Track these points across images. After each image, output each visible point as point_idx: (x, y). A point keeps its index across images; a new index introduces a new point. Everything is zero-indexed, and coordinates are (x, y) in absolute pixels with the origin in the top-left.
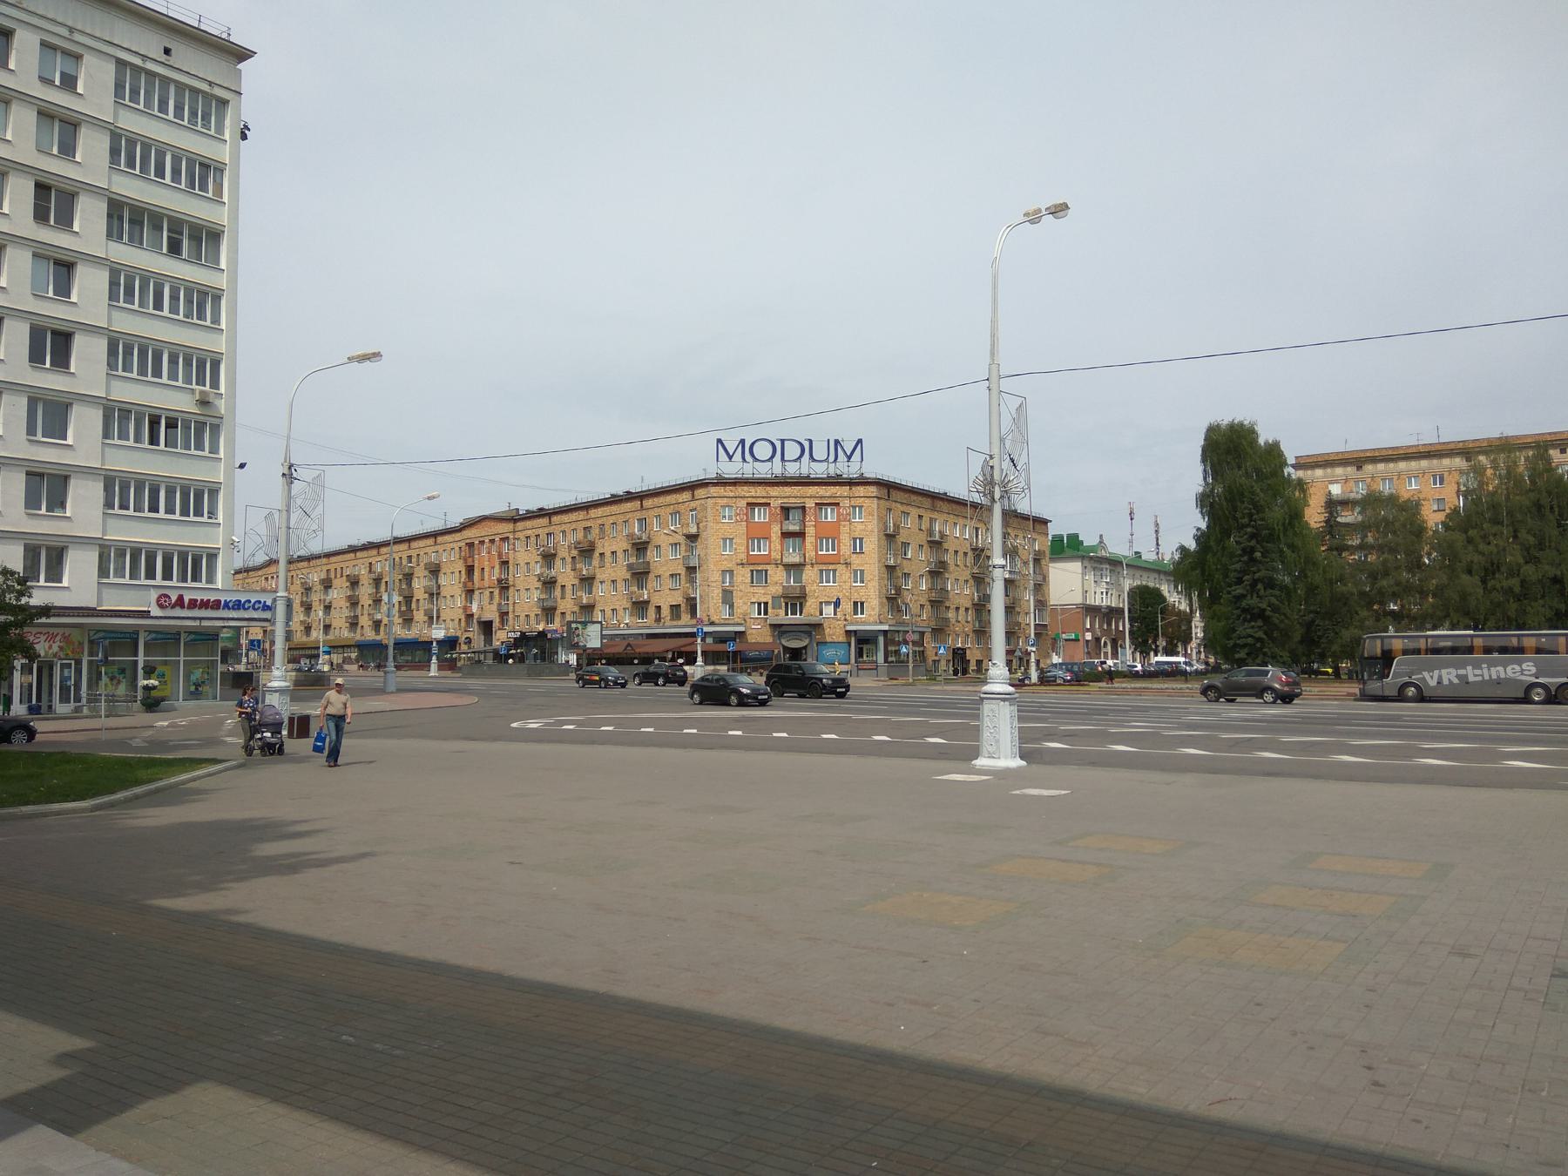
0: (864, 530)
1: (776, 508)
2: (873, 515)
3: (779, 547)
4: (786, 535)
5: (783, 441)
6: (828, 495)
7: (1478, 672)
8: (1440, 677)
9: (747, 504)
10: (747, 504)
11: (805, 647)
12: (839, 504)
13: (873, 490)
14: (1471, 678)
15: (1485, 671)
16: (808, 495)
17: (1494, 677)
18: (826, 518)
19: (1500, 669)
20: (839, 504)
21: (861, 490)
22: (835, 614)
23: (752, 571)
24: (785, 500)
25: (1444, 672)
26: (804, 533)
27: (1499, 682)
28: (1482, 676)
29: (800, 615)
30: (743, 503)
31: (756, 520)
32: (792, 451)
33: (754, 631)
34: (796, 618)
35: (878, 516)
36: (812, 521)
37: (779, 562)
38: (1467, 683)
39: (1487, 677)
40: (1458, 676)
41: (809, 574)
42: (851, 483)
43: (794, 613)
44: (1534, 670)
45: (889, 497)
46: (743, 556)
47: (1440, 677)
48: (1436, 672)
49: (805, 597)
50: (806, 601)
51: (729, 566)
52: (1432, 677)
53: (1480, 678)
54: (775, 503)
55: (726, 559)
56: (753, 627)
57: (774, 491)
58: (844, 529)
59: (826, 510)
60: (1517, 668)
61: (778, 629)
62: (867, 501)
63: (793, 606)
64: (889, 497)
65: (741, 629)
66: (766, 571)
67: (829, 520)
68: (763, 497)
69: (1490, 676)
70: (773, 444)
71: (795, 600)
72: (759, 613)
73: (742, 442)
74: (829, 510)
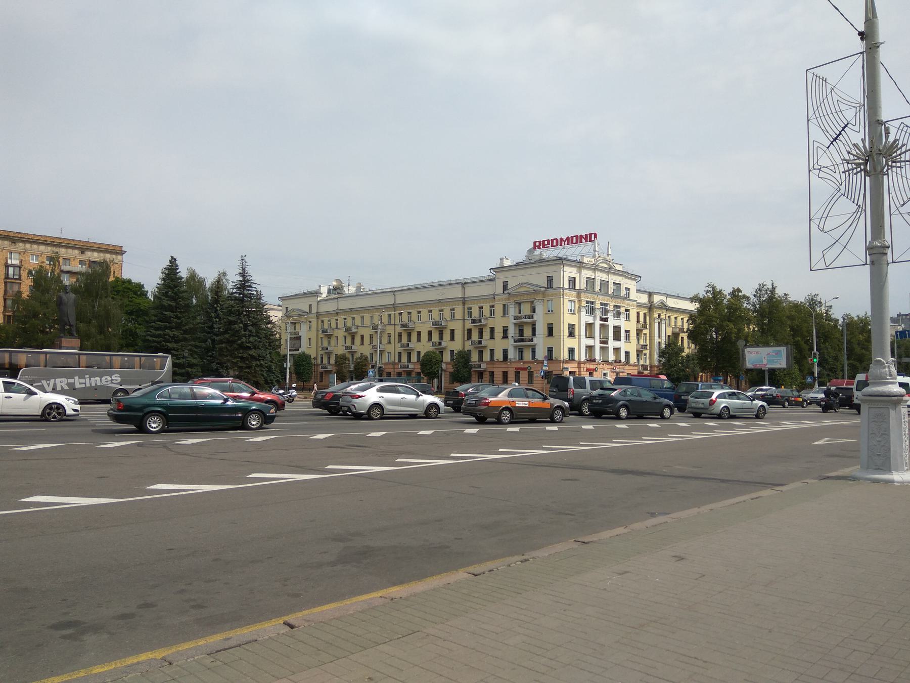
7: (82, 381)
8: (55, 384)
14: (78, 386)
15: (88, 380)
17: (93, 385)
19: (98, 379)
25: (58, 380)
27: (96, 388)
28: (85, 384)
38: (74, 389)
39: (88, 385)
40: (68, 384)
44: (119, 380)
47: (55, 384)
48: (52, 381)
52: (49, 385)
53: (83, 386)
60: (109, 379)
69: (91, 384)
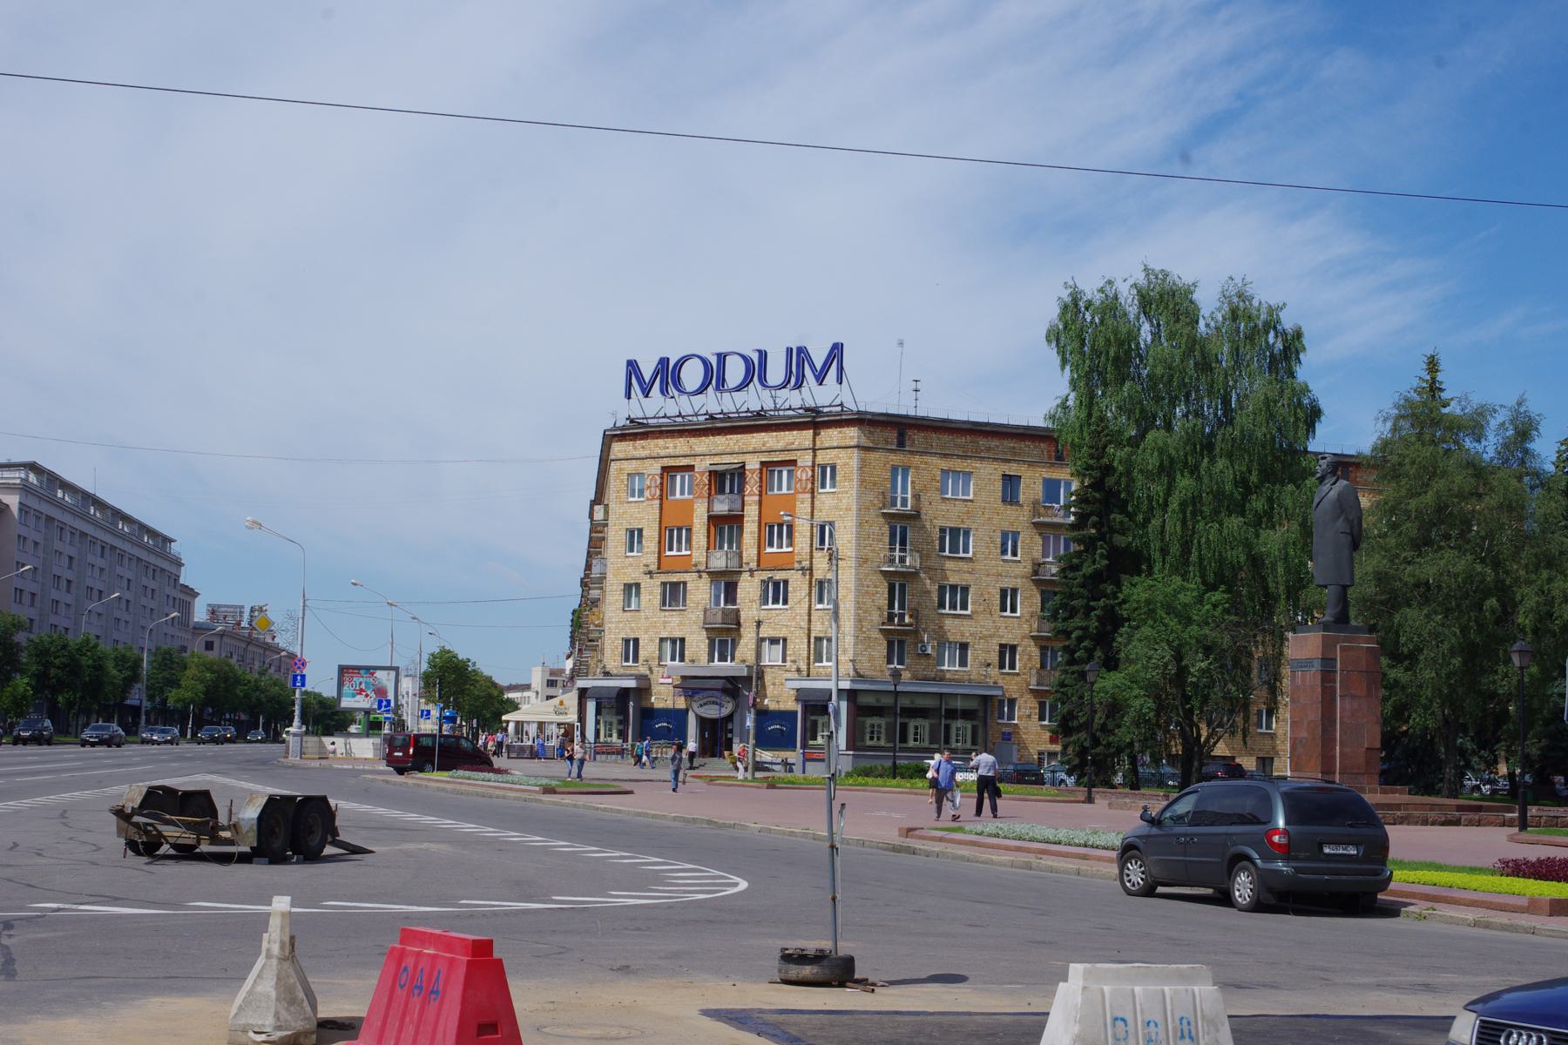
0: (837, 508)
1: (702, 474)
2: (851, 480)
3: (704, 542)
4: (715, 521)
5: (722, 358)
6: (780, 445)
9: (664, 468)
10: (664, 468)
11: (730, 718)
12: (795, 461)
13: (852, 434)
16: (751, 449)
18: (780, 488)
20: (795, 461)
21: (830, 436)
22: (784, 660)
23: (664, 584)
24: (717, 460)
26: (743, 516)
29: (733, 659)
30: (655, 468)
31: (678, 496)
32: (734, 373)
33: (662, 687)
34: (727, 668)
35: (862, 482)
36: (755, 495)
37: (702, 568)
41: (748, 588)
42: (815, 420)
43: (723, 658)
45: (901, 444)
46: (652, 560)
49: (738, 630)
50: (740, 636)
51: (633, 575)
54: (702, 465)
55: (631, 565)
56: (662, 681)
57: (702, 444)
58: (803, 507)
59: (780, 472)
61: (691, 687)
62: (842, 453)
63: (723, 643)
64: (901, 444)
65: (632, 684)
66: (685, 583)
67: (785, 491)
68: (685, 456)
70: (705, 362)
71: (724, 636)
72: (673, 659)
73: (664, 362)
74: (785, 474)
